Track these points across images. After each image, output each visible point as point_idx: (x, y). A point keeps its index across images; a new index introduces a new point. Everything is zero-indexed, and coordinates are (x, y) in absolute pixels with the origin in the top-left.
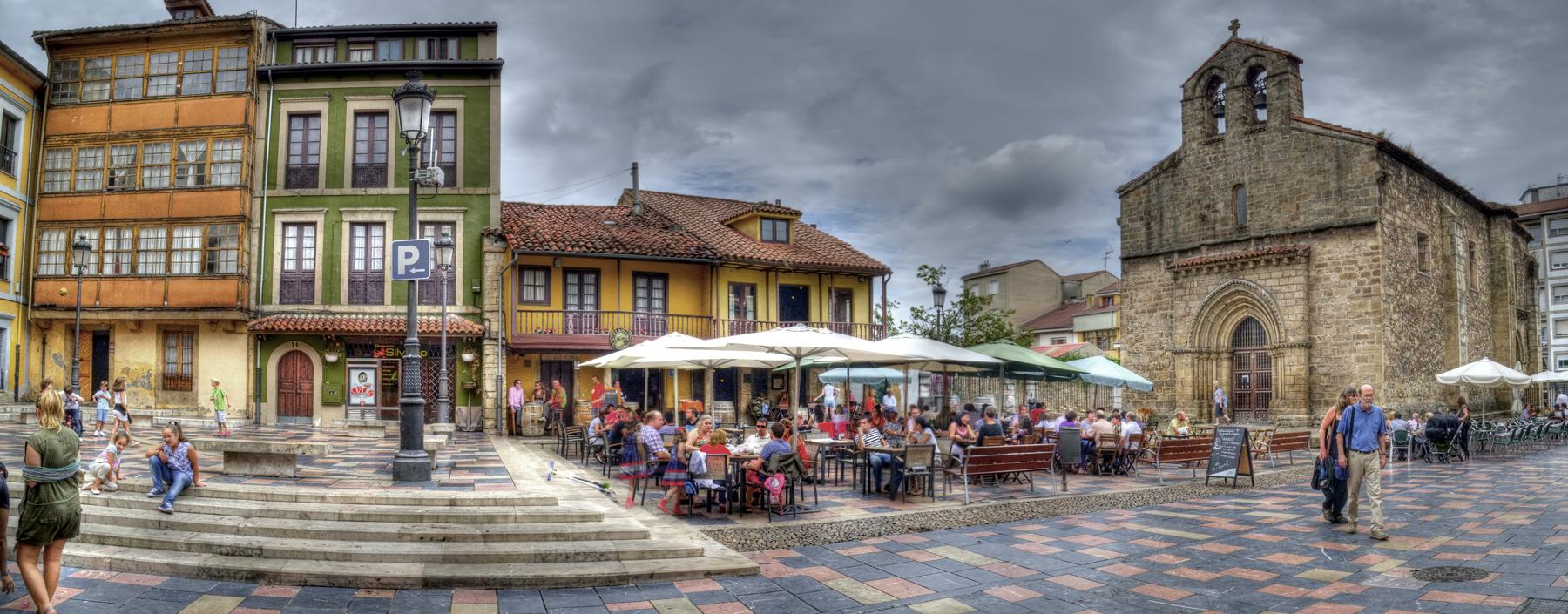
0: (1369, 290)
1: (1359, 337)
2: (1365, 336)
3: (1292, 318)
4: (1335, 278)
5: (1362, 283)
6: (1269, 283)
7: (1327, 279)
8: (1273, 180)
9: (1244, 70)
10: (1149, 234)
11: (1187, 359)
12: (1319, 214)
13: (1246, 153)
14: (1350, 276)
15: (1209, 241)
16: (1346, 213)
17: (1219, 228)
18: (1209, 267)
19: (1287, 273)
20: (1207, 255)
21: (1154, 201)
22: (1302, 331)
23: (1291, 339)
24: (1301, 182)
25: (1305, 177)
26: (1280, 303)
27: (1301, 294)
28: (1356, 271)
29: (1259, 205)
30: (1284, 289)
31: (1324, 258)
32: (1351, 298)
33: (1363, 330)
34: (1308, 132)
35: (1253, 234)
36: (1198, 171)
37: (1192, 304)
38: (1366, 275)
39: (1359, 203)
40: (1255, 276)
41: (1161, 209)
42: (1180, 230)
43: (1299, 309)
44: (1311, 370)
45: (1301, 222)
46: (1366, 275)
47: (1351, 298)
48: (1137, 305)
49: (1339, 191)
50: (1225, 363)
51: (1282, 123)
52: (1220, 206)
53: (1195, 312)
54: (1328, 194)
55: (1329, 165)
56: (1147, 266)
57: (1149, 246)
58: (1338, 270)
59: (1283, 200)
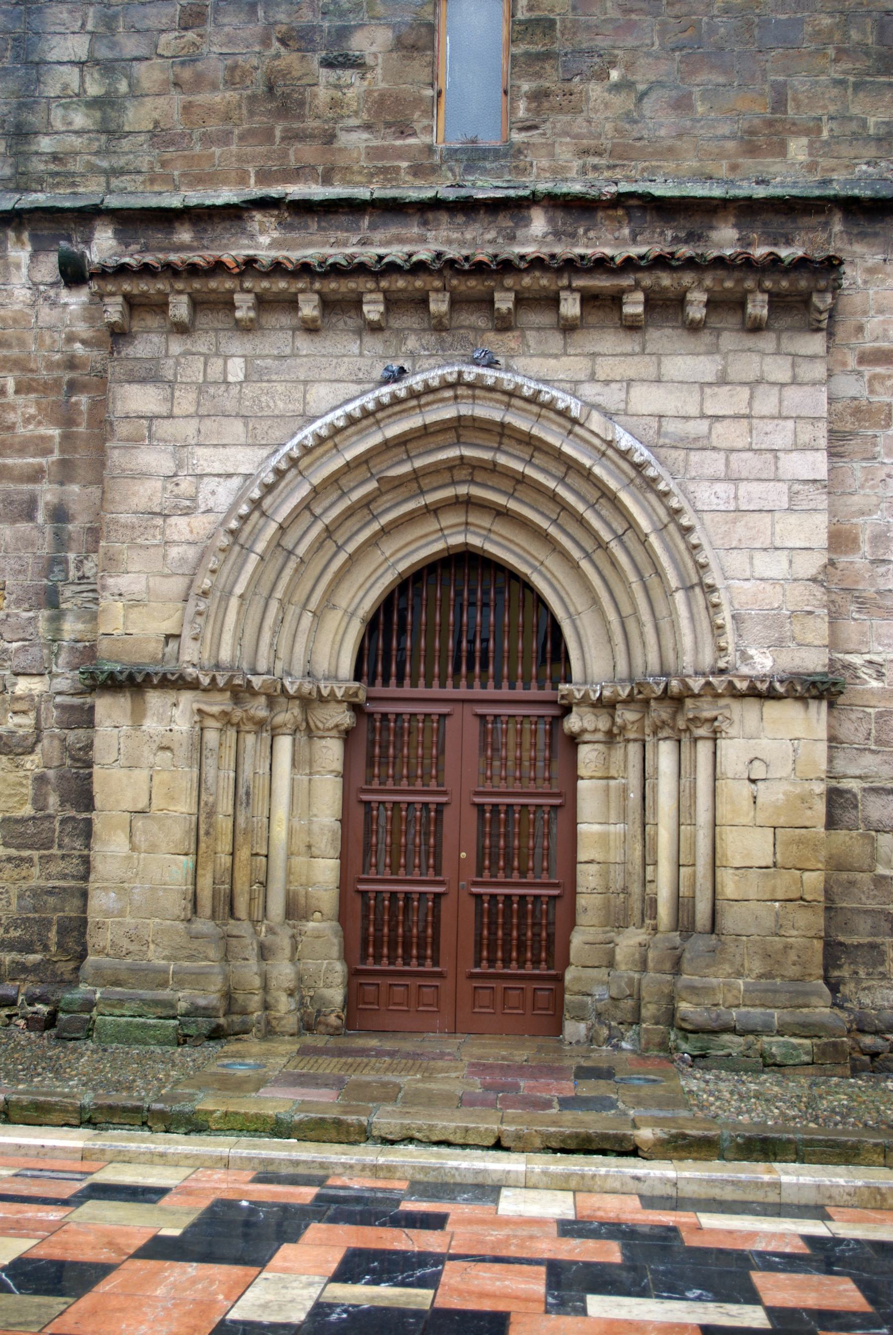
3: (773, 566)
6: (647, 400)
11: (171, 717)
18: (340, 295)
19: (746, 366)
20: (264, 241)
22: (818, 630)
23: (763, 662)
26: (710, 496)
27: (817, 464)
30: (728, 434)
37: (206, 459)
40: (570, 366)
42: (138, 117)
43: (812, 530)
44: (838, 803)
50: (331, 752)
53: (220, 496)
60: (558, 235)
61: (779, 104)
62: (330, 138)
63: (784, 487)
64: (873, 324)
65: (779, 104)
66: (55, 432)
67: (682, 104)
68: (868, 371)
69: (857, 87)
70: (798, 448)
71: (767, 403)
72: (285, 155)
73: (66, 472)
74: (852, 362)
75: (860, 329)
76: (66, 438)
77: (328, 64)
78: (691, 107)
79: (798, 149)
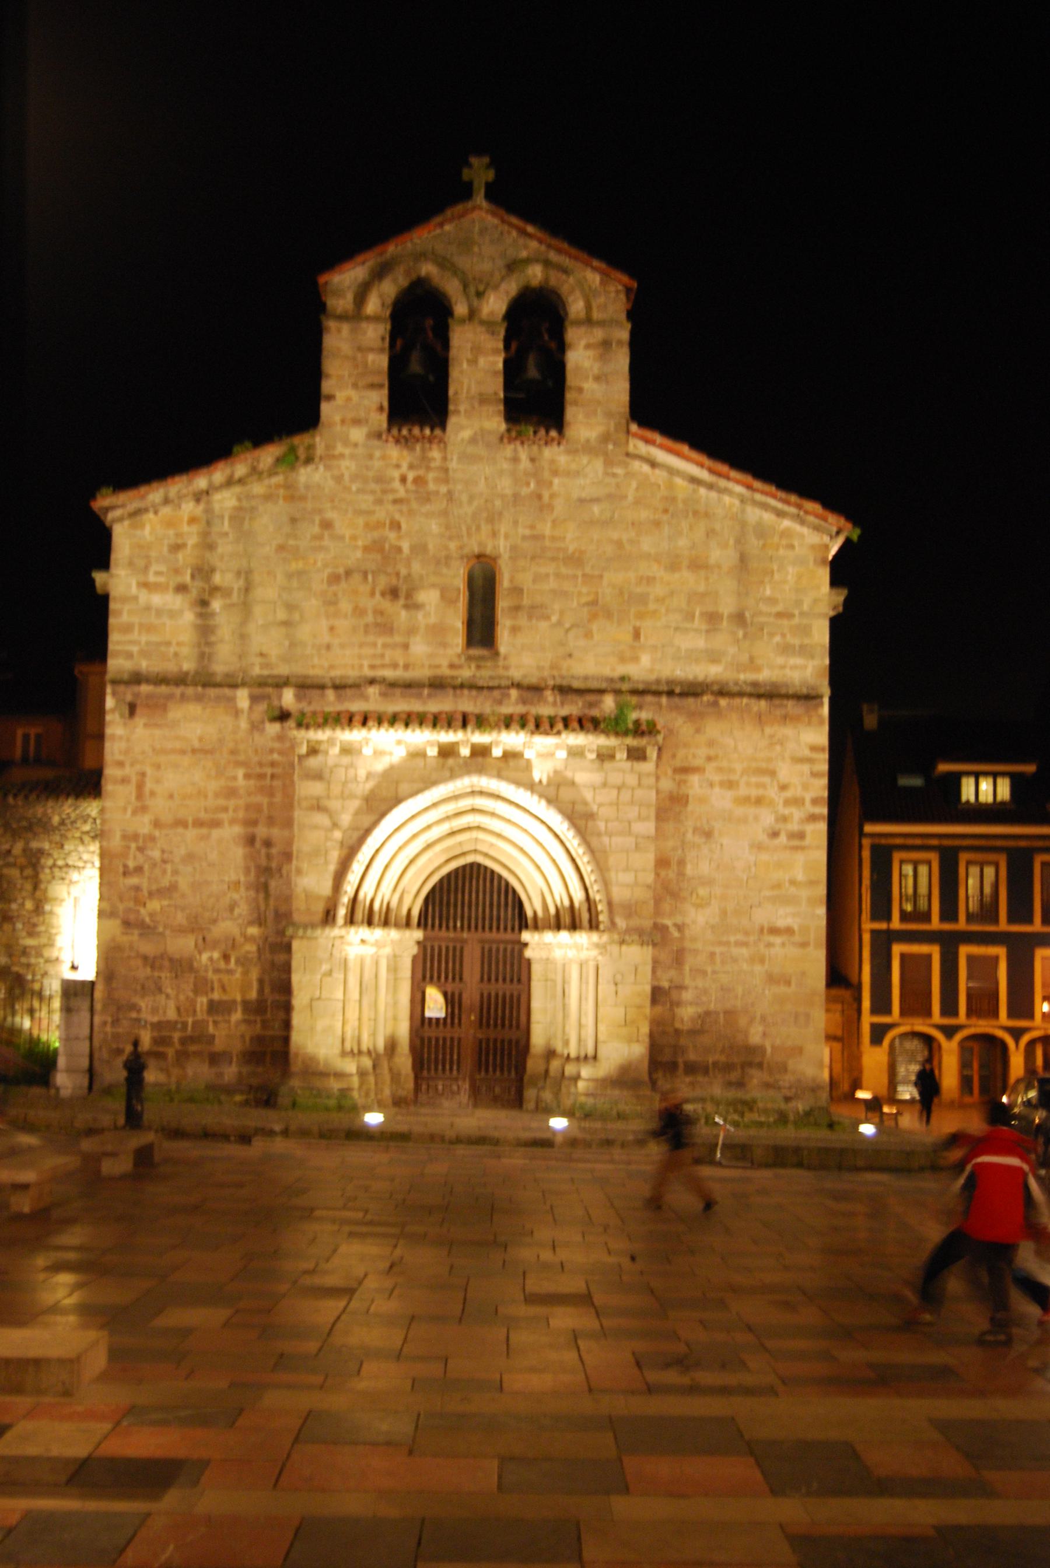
0: (801, 836)
1: (774, 931)
2: (789, 931)
4: (721, 800)
5: (784, 819)
7: (703, 800)
8: (576, 560)
9: (511, 288)
10: (205, 630)
12: (692, 656)
13: (505, 485)
14: (759, 801)
15: (389, 674)
16: (752, 664)
17: (419, 648)
21: (225, 547)
24: (650, 580)
25: (656, 570)
28: (772, 792)
29: (537, 611)
31: (698, 755)
32: (759, 847)
33: (784, 917)
34: (672, 471)
35: (516, 674)
36: (366, 501)
38: (798, 802)
39: (786, 649)
41: (246, 575)
45: (644, 668)
46: (798, 802)
47: (759, 847)
48: (159, 806)
49: (739, 618)
51: (605, 438)
52: (429, 597)
54: (713, 618)
55: (721, 555)
56: (194, 709)
57: (204, 658)
58: (730, 785)
59: (596, 609)
60: (524, 702)
61: (637, 635)
62: (406, 646)
63: (632, 840)
64: (681, 753)
65: (637, 635)
66: (265, 801)
67: (589, 635)
68: (677, 777)
69: (676, 629)
70: (640, 818)
71: (626, 796)
72: (382, 656)
73: (271, 821)
74: (670, 772)
75: (674, 756)
76: (271, 804)
77: (407, 607)
78: (592, 637)
79: (645, 660)
